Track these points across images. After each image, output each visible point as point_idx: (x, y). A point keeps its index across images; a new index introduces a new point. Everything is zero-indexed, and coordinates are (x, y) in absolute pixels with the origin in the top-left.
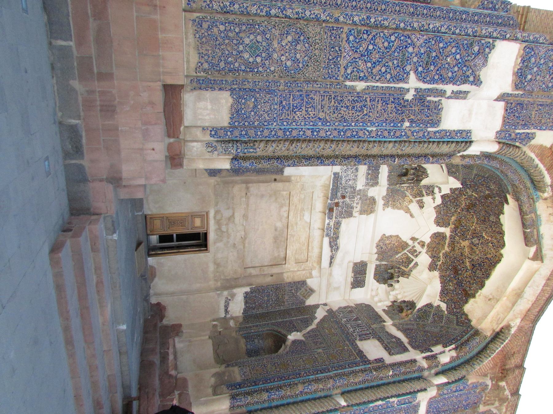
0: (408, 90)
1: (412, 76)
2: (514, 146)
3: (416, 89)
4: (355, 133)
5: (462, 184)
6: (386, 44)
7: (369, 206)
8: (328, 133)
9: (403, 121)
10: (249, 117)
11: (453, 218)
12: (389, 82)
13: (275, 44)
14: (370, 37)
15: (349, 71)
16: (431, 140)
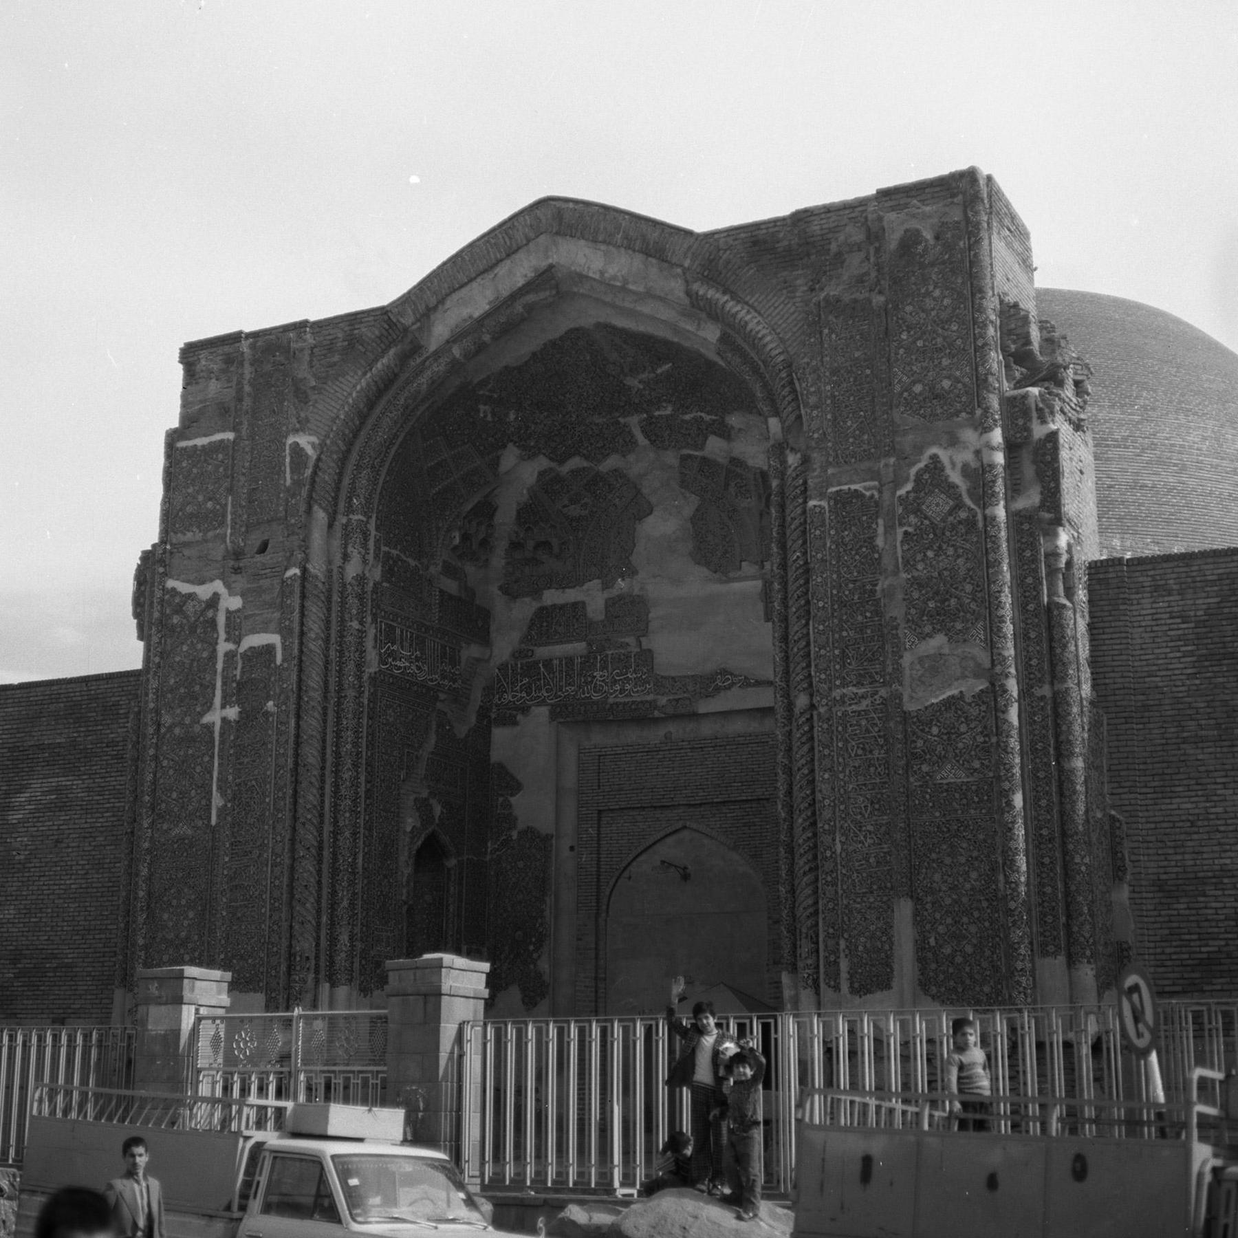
0: (224, 720)
1: (207, 719)
2: (315, 473)
3: (223, 707)
4: (280, 794)
5: (504, 446)
6: (171, 772)
7: (629, 612)
8: (279, 838)
9: (267, 714)
10: (254, 966)
11: (599, 420)
12: (212, 757)
13: (171, 936)
14: (164, 797)
15: (200, 823)
16: (296, 652)
